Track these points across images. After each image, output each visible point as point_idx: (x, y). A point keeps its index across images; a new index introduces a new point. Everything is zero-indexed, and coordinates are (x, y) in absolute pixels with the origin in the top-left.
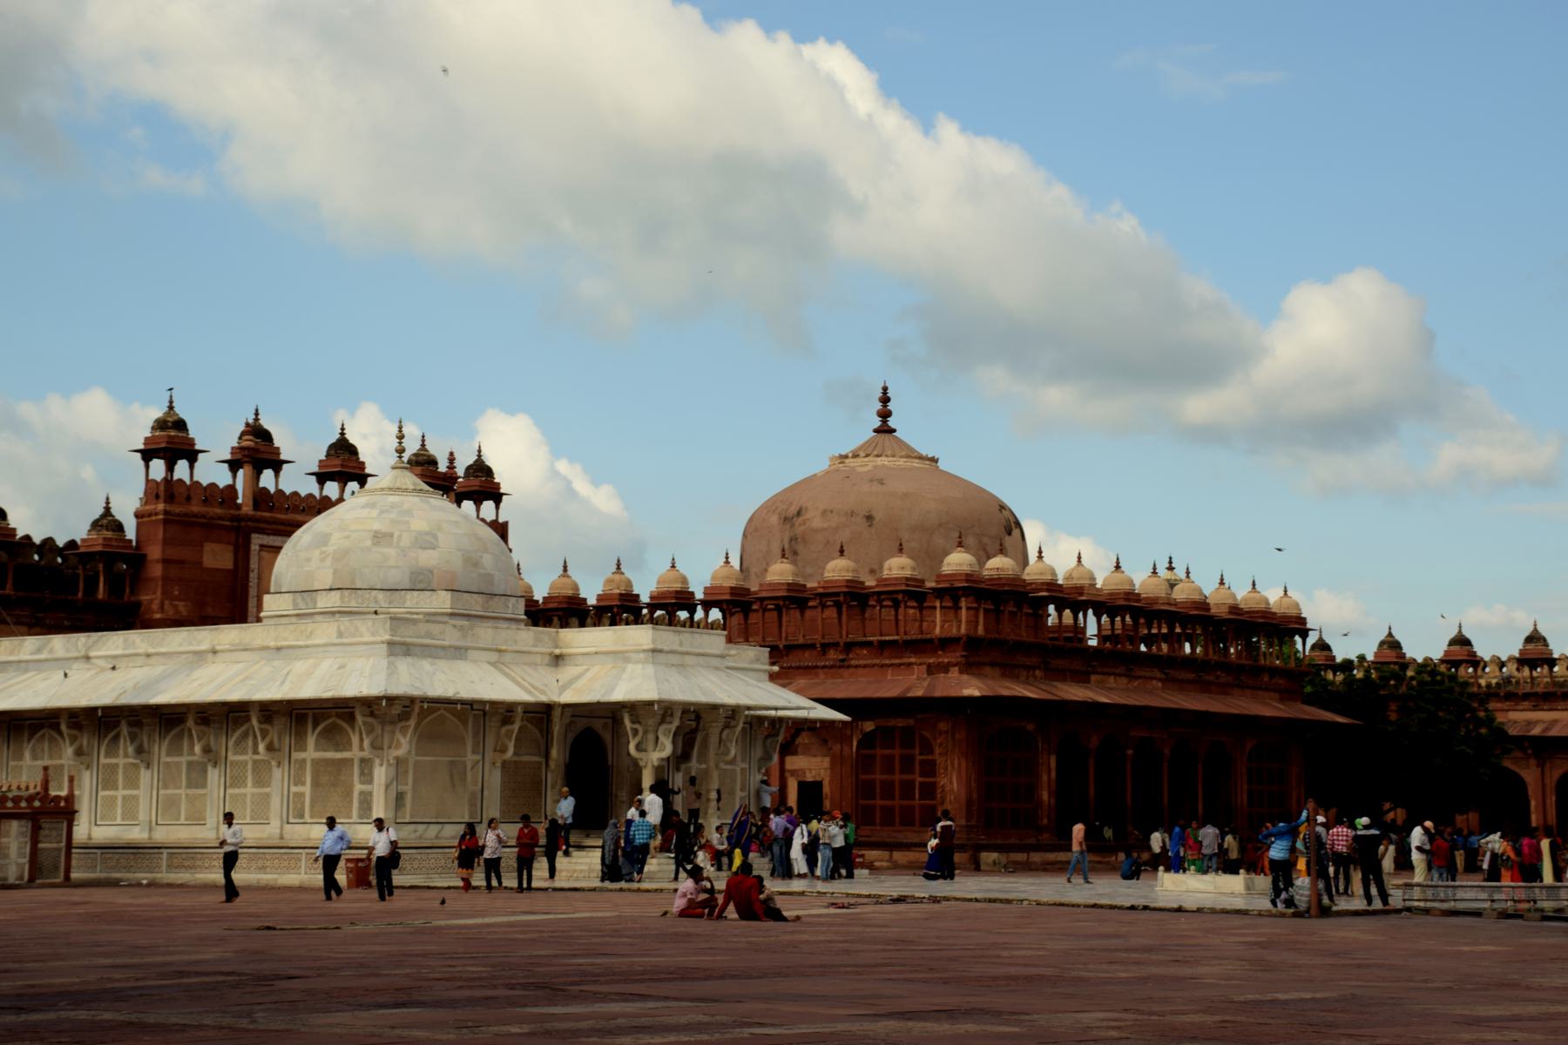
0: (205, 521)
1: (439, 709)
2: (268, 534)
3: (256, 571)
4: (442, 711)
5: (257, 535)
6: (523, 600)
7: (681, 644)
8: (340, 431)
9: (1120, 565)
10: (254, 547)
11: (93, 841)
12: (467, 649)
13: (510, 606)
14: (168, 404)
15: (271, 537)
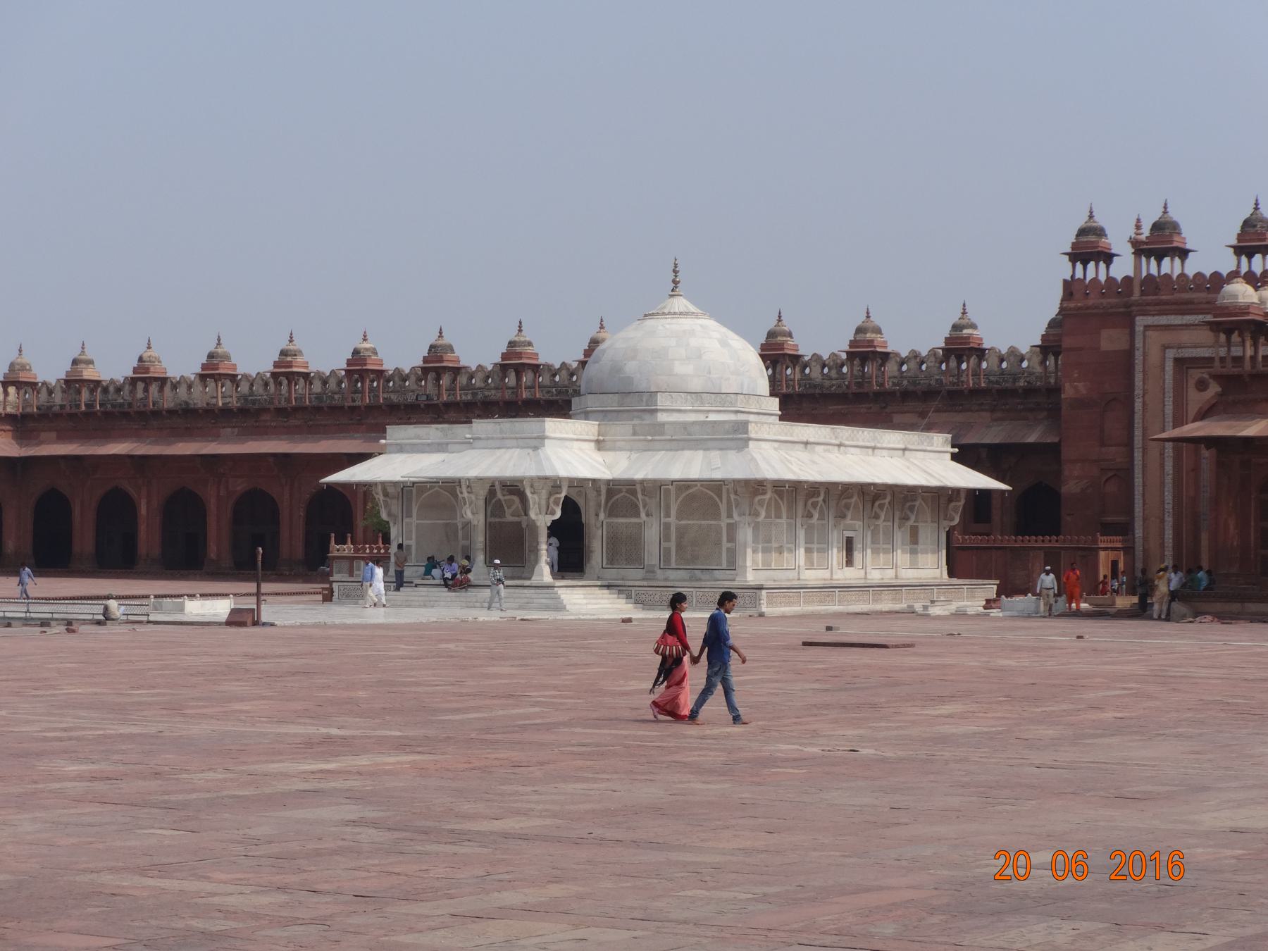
0: (1102, 311)
1: (435, 487)
2: (1153, 315)
3: (1141, 349)
4: (435, 489)
5: (1141, 318)
6: (1242, 355)
7: (502, 431)
8: (1255, 206)
9: (967, 311)
10: (1139, 329)
11: (869, 581)
12: (447, 444)
13: (644, 400)
14: (1089, 214)
15: (1156, 318)
